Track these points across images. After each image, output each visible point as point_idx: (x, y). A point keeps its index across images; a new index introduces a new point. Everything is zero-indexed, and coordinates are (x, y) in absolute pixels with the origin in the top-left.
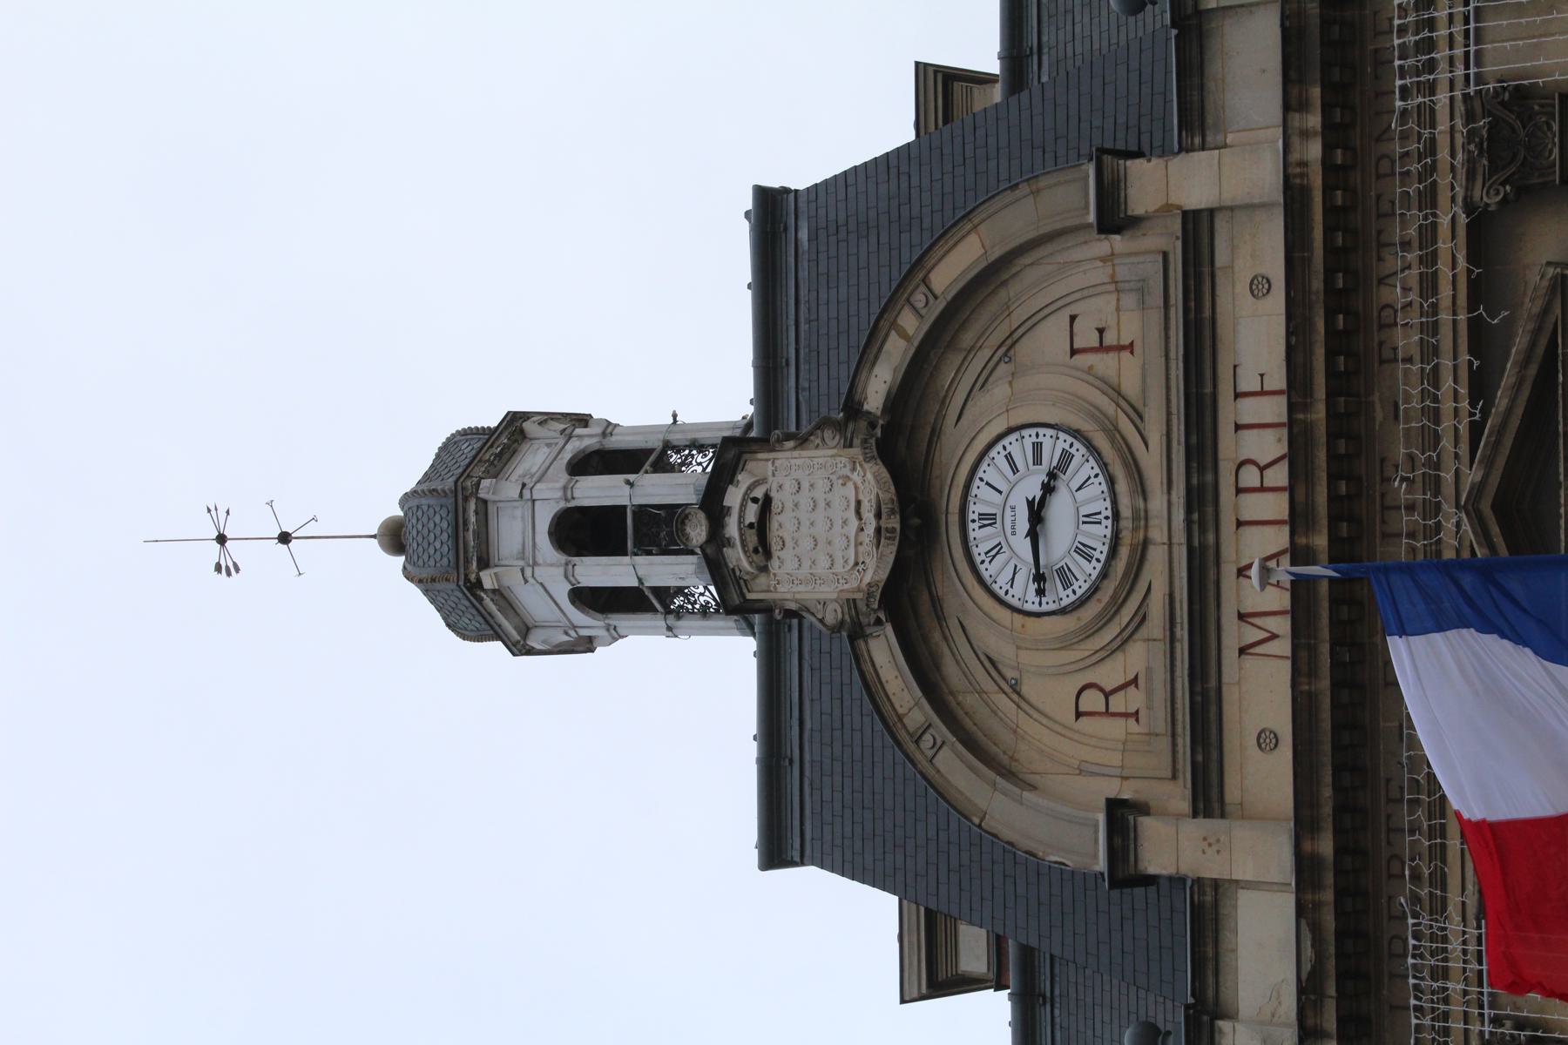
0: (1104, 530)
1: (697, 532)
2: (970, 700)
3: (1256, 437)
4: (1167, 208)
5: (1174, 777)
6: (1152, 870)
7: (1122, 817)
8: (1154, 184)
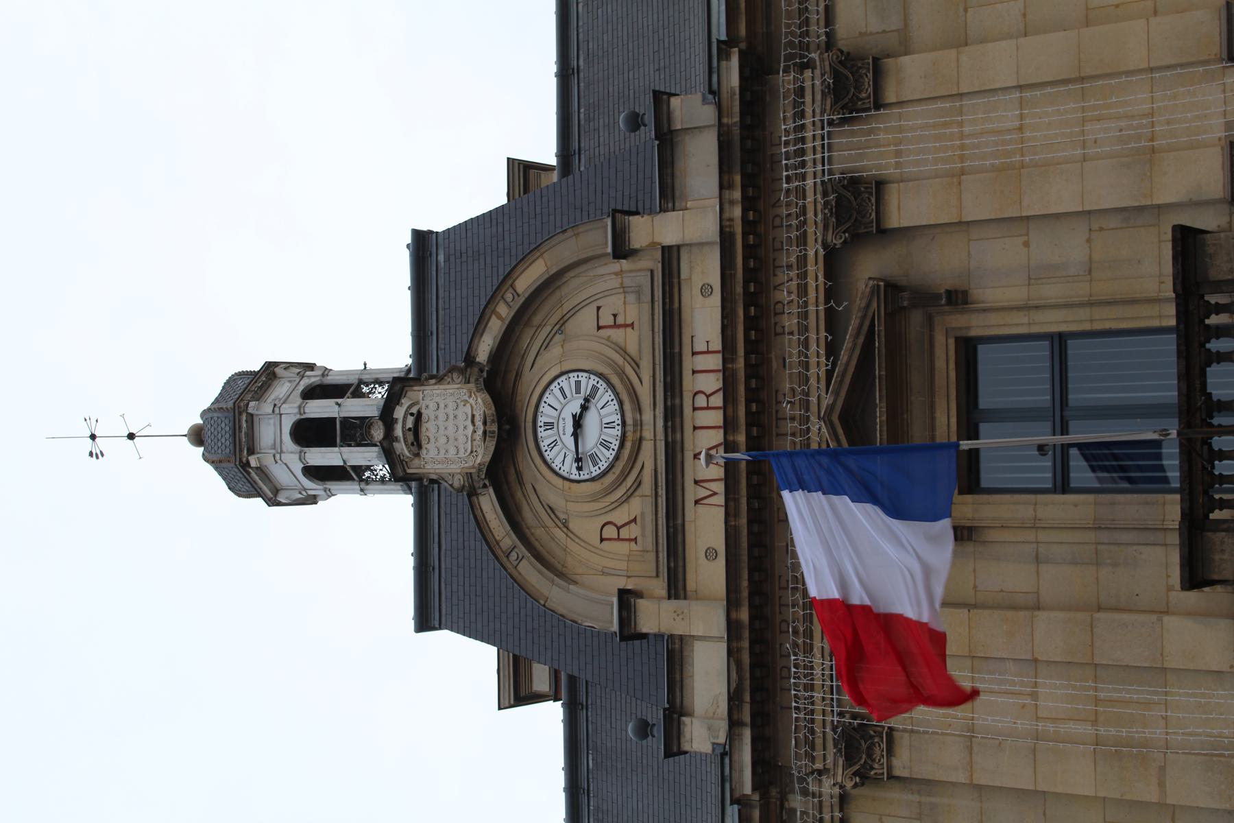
0: (617, 432)
1: (378, 433)
2: (539, 532)
3: (704, 378)
4: (653, 245)
5: (657, 576)
6: (644, 630)
7: (626, 599)
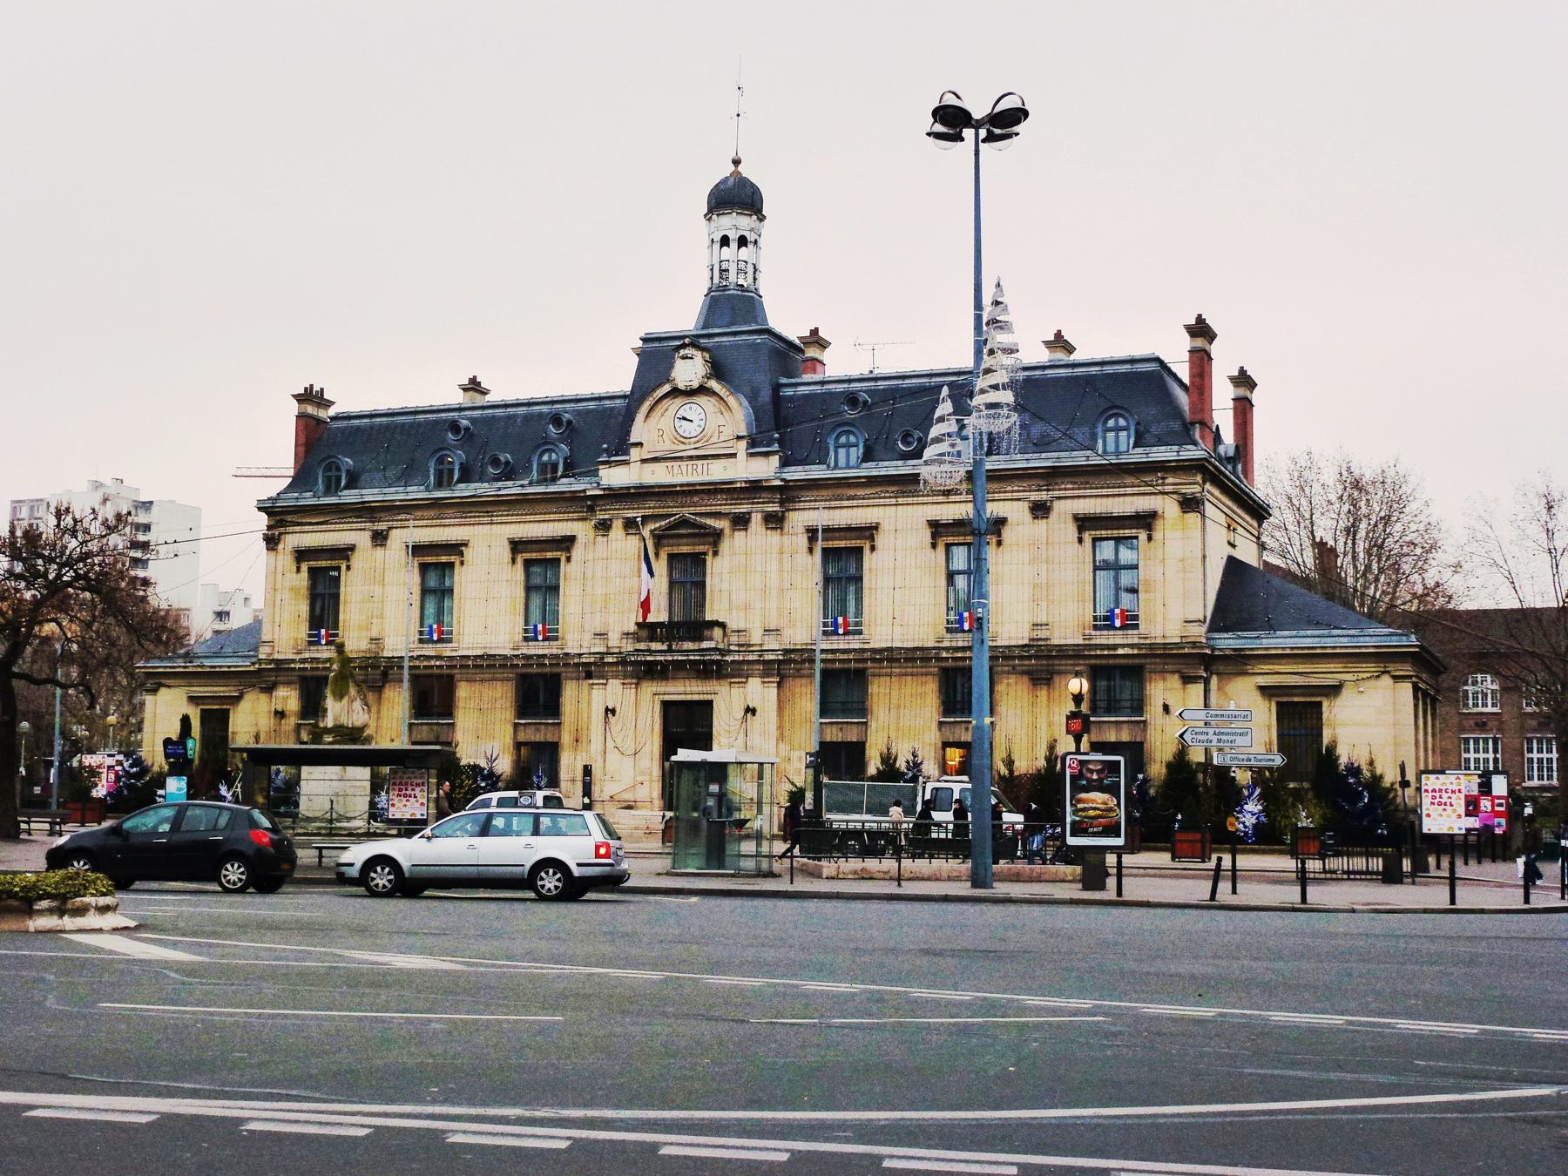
7: (640, 444)
8: (743, 444)
